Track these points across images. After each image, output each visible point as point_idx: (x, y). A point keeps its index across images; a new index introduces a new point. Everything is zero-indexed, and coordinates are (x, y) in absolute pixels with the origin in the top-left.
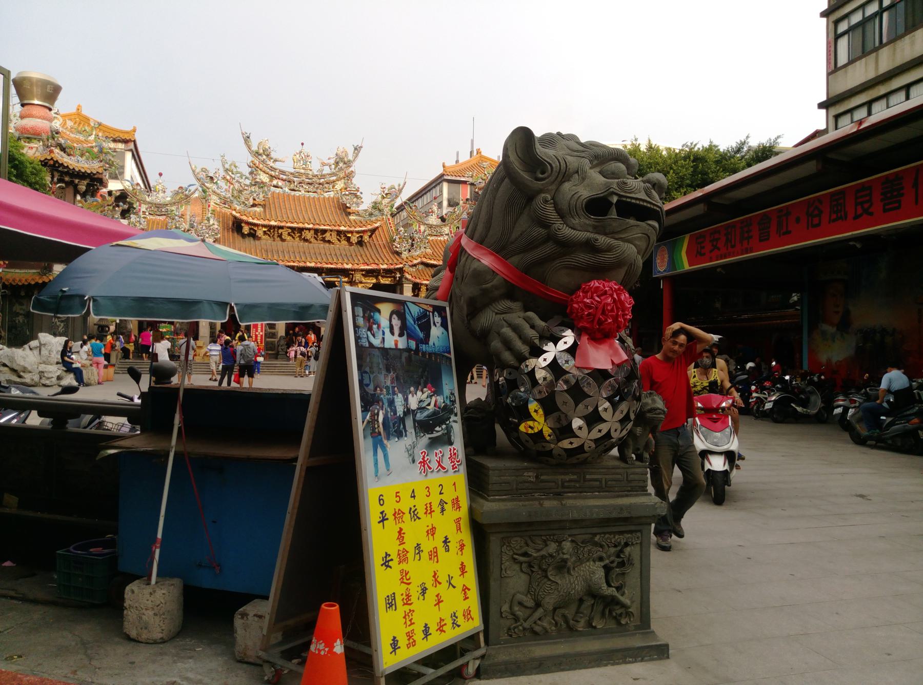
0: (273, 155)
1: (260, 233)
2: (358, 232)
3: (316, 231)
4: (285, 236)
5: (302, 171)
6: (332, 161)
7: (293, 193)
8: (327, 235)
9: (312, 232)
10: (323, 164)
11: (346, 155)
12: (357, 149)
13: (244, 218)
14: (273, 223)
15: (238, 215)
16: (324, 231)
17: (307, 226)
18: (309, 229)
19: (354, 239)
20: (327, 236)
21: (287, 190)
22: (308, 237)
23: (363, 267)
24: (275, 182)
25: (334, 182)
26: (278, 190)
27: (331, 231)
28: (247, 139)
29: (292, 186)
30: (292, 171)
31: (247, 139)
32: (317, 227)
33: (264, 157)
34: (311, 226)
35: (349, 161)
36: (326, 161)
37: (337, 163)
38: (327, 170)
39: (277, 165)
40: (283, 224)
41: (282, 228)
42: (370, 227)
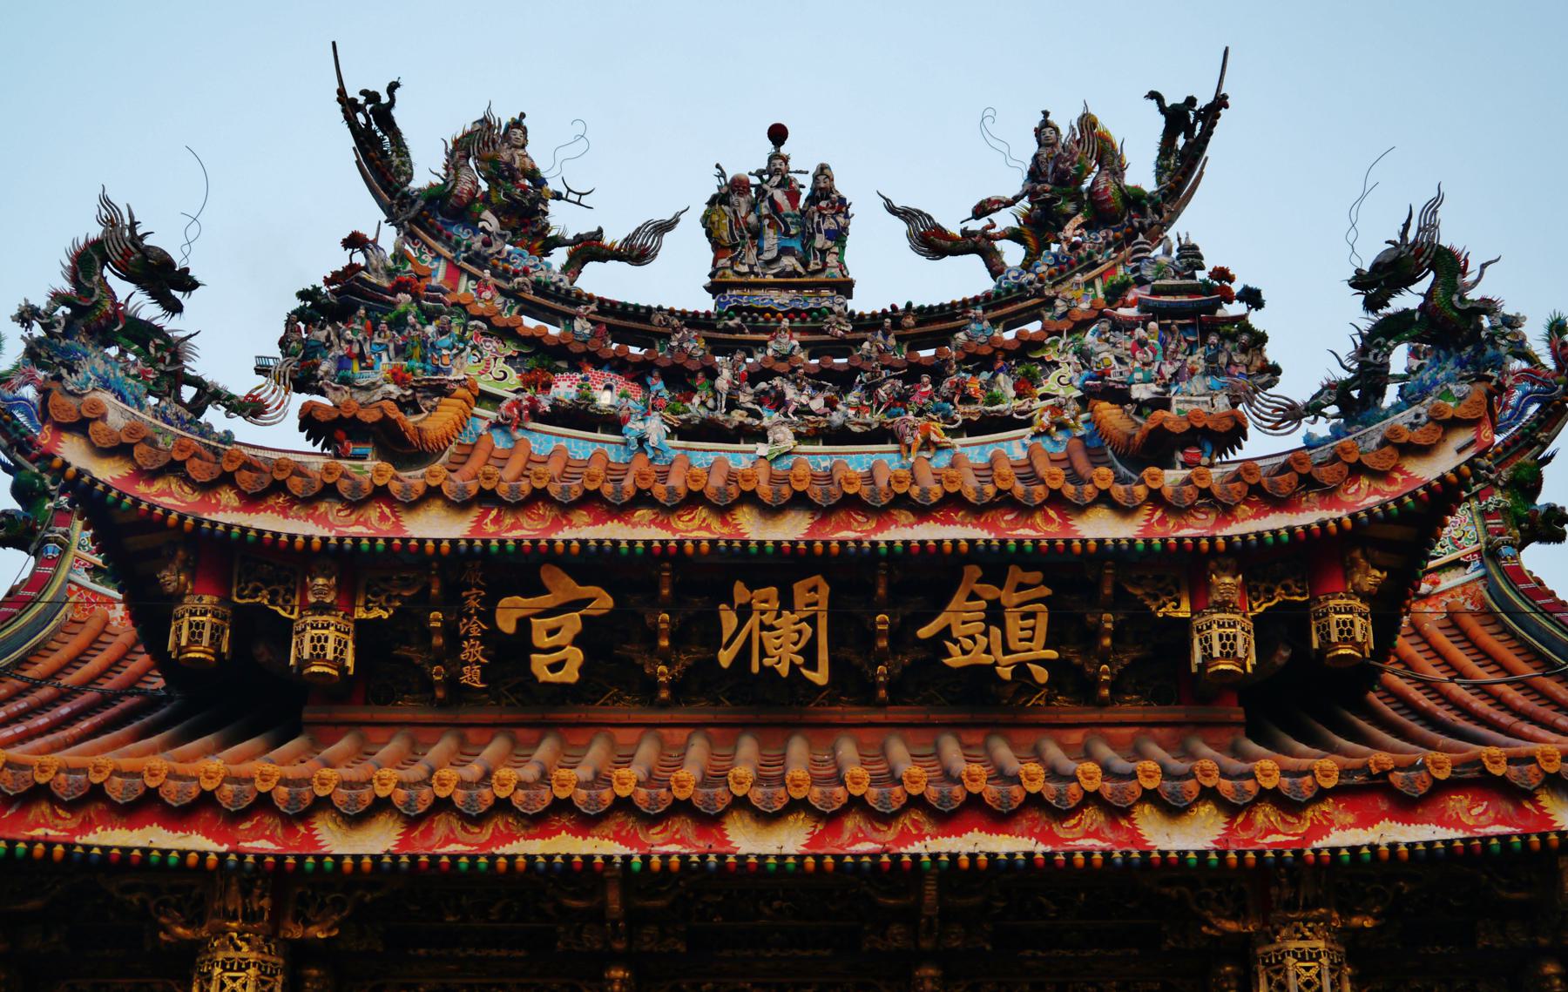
0: (563, 220)
1: (323, 640)
2: (1255, 560)
3: (851, 574)
4: (558, 657)
5: (780, 299)
6: (1005, 219)
7: (704, 455)
8: (960, 617)
9: (814, 594)
10: (933, 242)
11: (1108, 155)
12: (1188, 128)
13: (170, 497)
14: (433, 526)
15: (107, 472)
16: (932, 575)
17: (753, 528)
18: (780, 568)
19: (1226, 636)
20: (964, 633)
21: (655, 428)
22: (781, 653)
23: (1345, 836)
24: (564, 389)
25: (1028, 346)
26: (580, 445)
27: (995, 563)
28: (373, 129)
29: (696, 408)
30: (705, 303)
31: (373, 129)
32: (850, 532)
33: (490, 222)
34: (792, 529)
35: (1134, 199)
36: (953, 219)
37: (1038, 229)
38: (964, 278)
39: (599, 280)
40: (526, 530)
41: (520, 570)
42: (1366, 497)
